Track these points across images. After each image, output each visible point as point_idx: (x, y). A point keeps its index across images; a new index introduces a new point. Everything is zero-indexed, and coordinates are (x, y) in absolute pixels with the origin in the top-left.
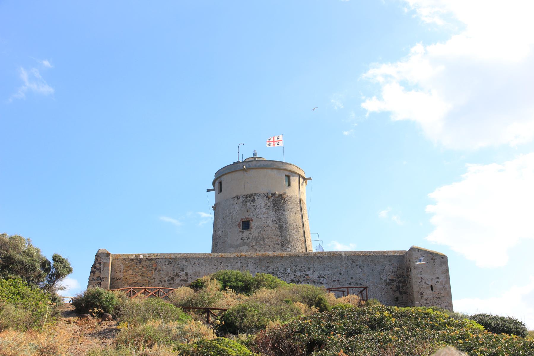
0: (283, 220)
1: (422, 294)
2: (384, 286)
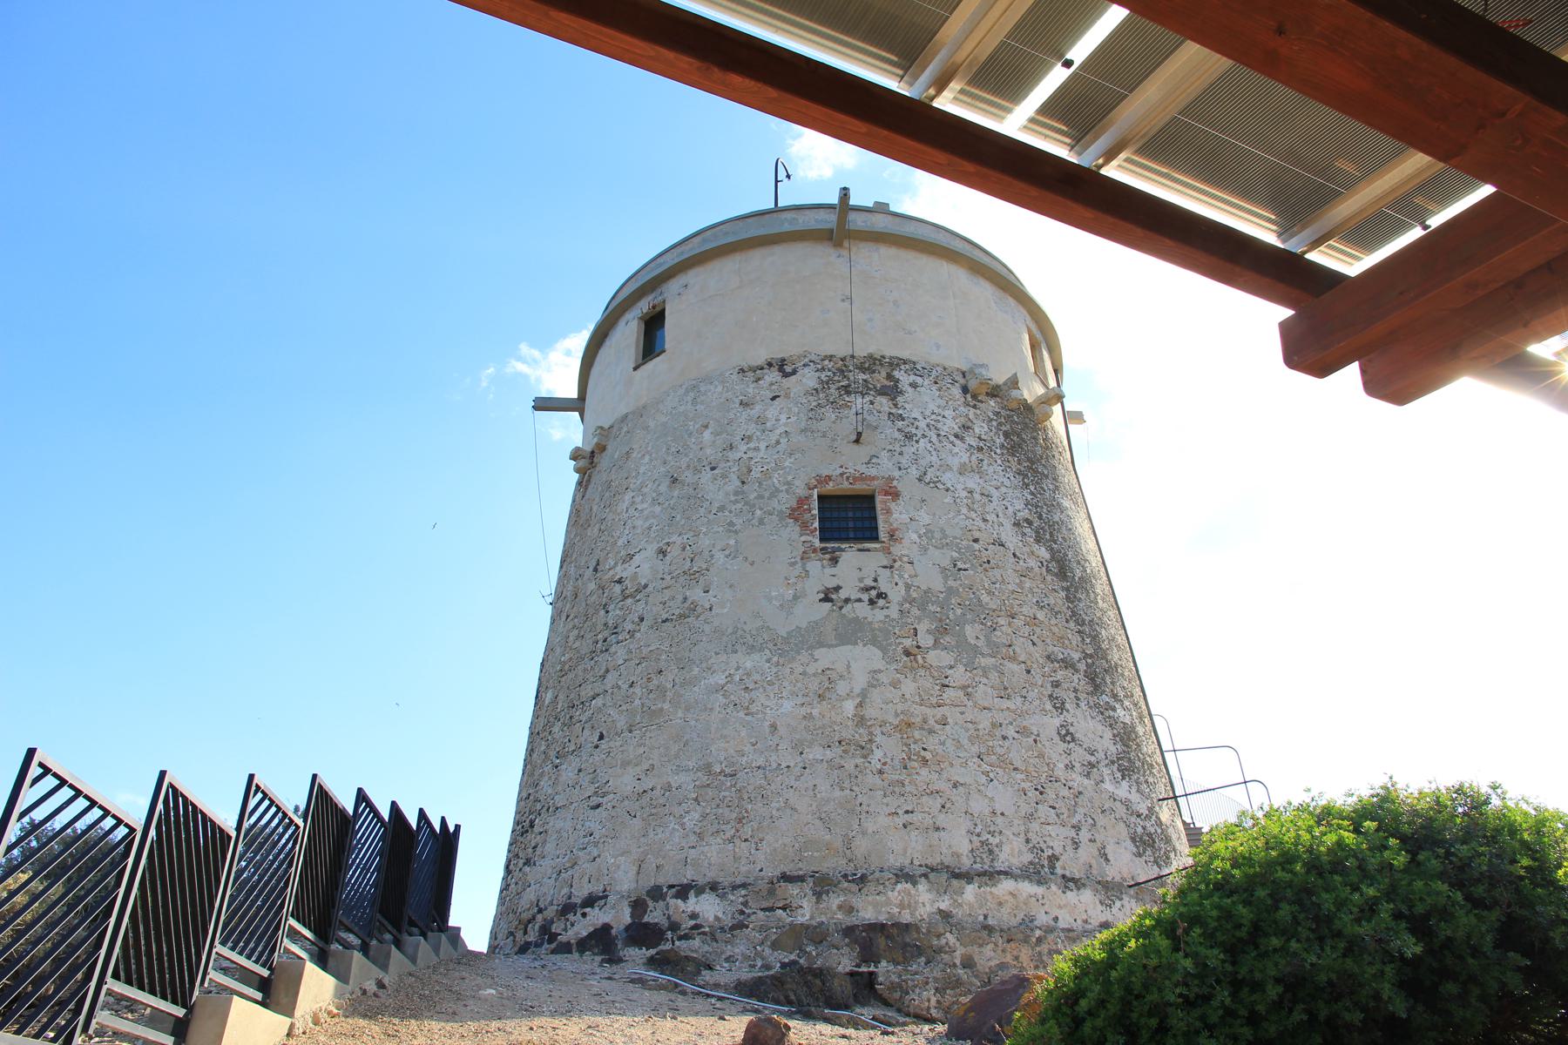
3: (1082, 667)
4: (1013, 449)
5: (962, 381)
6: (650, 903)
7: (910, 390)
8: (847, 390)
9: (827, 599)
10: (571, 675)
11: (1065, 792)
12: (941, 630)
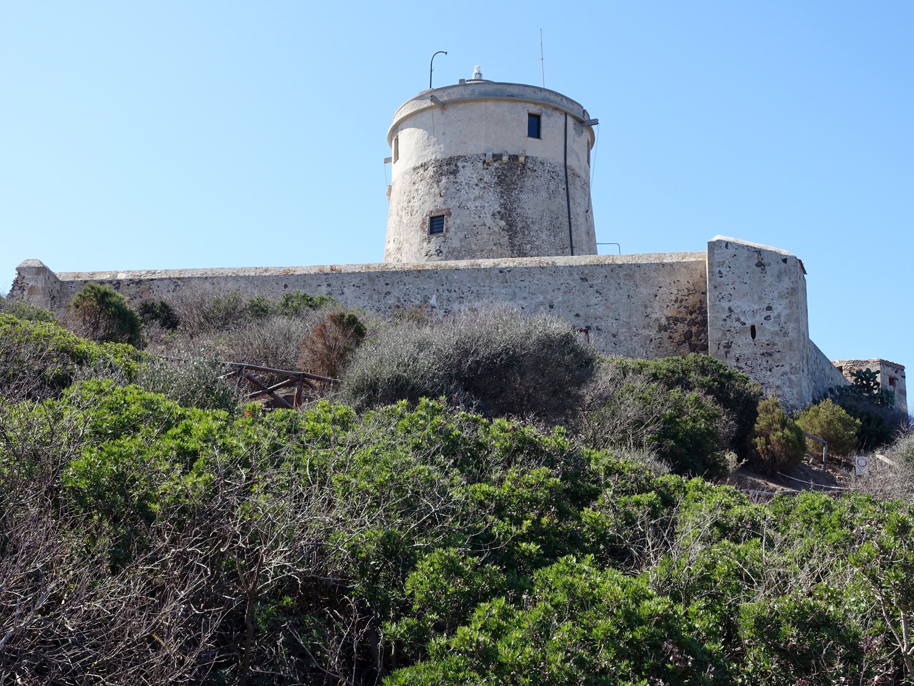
0: (519, 210)
1: (728, 346)
2: (653, 333)
8: (441, 174)
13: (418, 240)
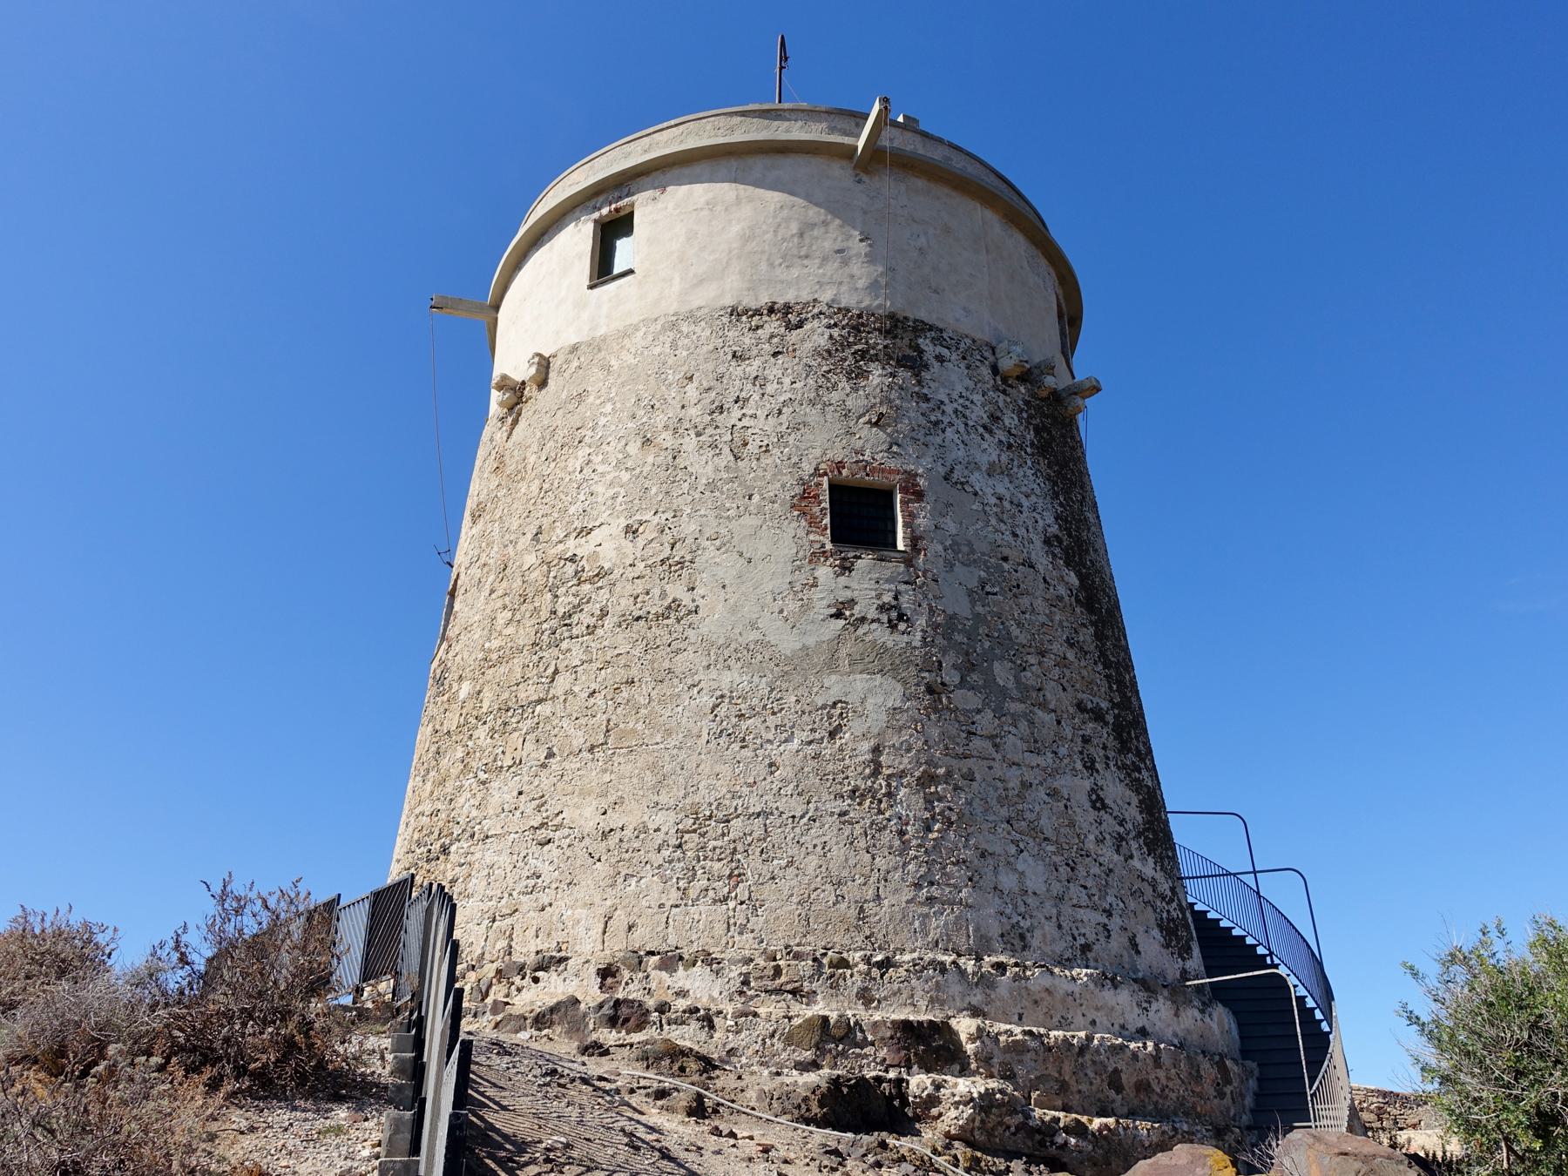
3: (1110, 719)
4: (1043, 449)
5: (992, 359)
6: (626, 974)
7: (937, 365)
9: (838, 615)
10: (503, 669)
11: (1096, 870)
12: (968, 667)
13: (787, 549)
